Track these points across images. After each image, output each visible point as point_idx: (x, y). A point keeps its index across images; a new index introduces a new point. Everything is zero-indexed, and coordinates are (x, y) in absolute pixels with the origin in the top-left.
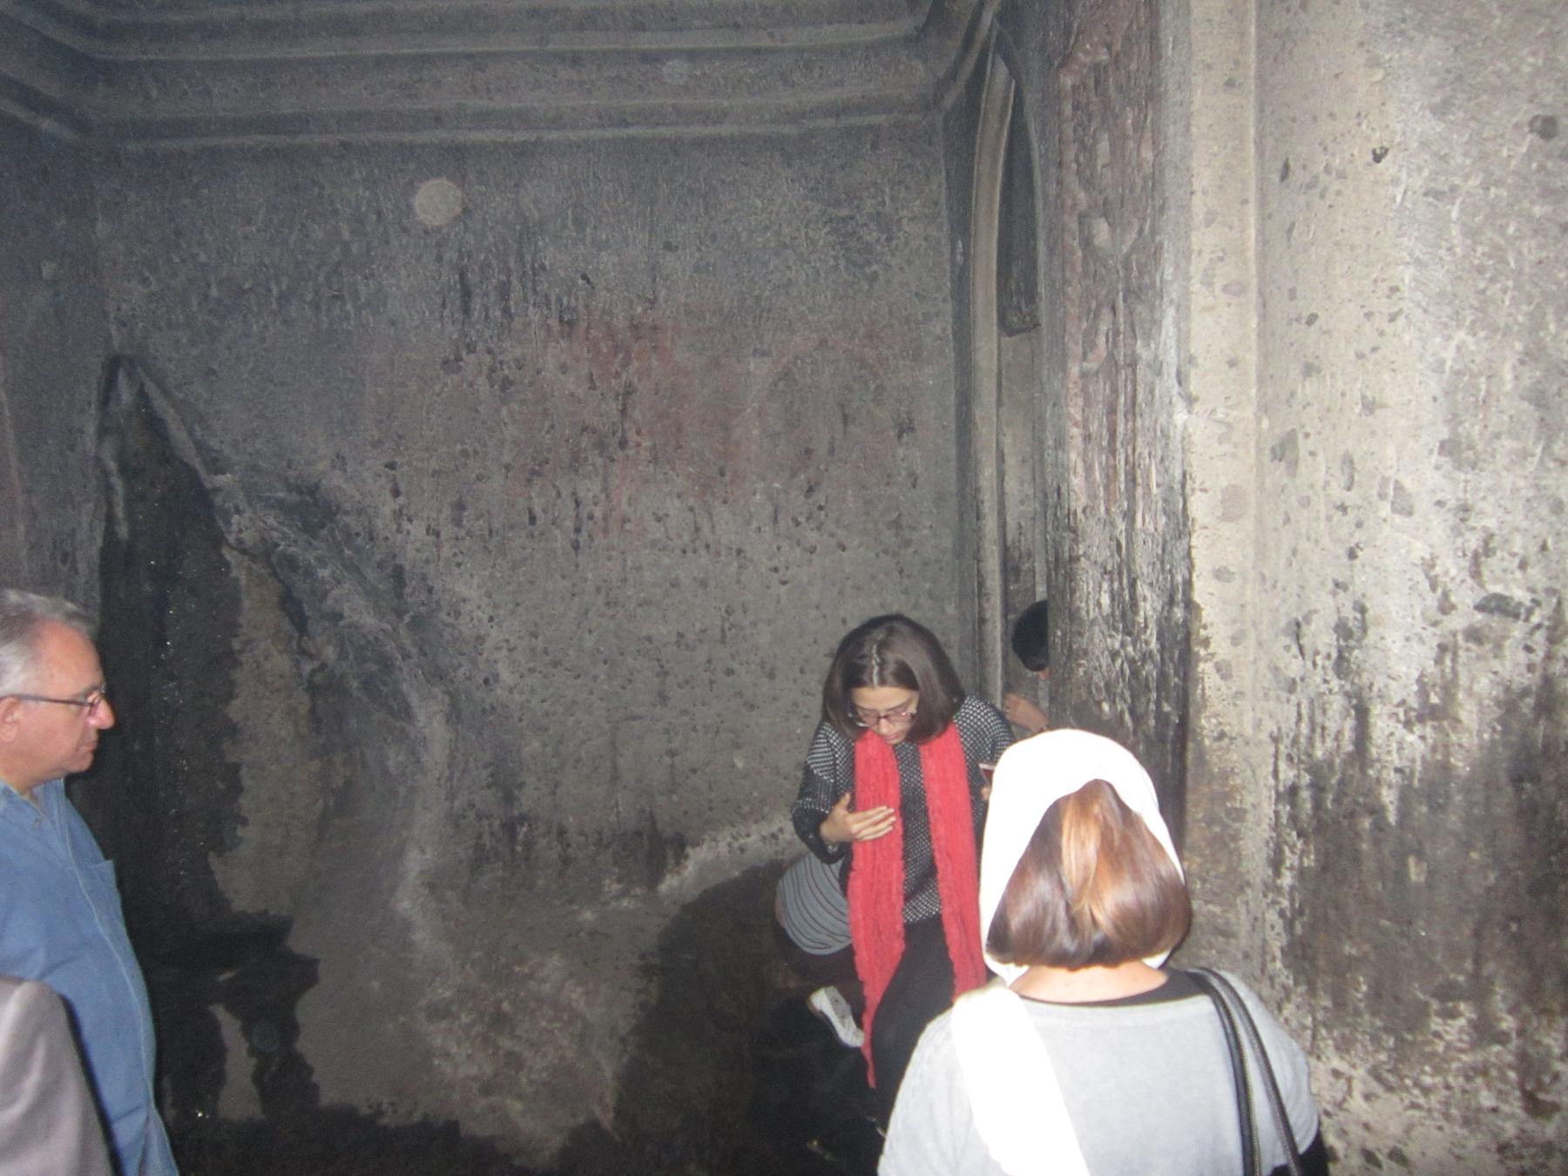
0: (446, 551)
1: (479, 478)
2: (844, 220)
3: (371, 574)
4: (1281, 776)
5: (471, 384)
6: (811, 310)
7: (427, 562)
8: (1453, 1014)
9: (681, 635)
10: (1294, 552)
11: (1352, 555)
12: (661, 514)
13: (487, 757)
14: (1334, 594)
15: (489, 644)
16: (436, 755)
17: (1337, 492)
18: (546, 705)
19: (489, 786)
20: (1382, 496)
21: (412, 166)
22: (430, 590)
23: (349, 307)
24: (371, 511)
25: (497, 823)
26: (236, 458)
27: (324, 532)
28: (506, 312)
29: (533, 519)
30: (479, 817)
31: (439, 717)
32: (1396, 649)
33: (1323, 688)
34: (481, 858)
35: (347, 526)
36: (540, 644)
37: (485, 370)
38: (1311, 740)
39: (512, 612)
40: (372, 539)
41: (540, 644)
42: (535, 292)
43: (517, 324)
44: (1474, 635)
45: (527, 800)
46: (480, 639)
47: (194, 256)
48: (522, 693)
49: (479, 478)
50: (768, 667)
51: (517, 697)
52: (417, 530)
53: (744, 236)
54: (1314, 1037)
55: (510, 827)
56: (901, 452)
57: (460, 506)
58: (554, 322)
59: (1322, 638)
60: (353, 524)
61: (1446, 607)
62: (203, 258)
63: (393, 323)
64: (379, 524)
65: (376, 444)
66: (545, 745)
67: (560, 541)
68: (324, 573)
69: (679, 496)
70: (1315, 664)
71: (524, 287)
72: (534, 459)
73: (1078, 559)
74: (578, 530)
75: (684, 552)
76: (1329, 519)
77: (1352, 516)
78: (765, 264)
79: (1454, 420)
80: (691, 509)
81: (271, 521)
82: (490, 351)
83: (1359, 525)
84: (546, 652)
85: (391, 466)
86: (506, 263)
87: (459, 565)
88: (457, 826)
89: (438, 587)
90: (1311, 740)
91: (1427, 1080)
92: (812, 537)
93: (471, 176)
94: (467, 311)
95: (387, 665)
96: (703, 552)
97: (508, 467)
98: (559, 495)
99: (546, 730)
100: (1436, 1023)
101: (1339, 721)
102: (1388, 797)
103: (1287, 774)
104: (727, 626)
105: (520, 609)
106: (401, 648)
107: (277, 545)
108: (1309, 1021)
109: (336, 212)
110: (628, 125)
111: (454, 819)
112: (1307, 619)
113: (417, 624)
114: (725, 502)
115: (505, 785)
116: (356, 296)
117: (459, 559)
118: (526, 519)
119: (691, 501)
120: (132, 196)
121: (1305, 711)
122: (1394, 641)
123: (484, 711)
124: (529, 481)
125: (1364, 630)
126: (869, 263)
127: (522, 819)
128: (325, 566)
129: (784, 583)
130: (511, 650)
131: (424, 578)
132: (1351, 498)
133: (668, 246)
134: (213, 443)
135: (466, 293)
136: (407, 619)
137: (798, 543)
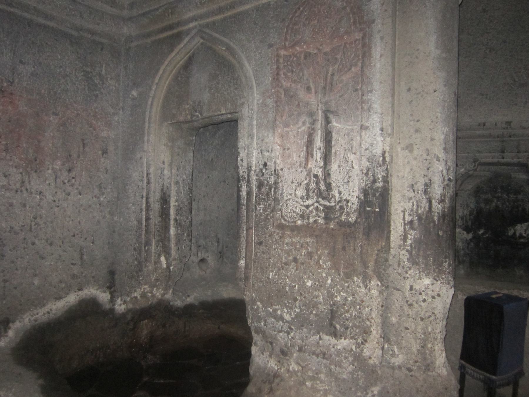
2: (88, 72)
4: (406, 219)
6: (75, 102)
8: (446, 262)
9: (12, 228)
10: (411, 170)
11: (428, 169)
12: (7, 174)
14: (424, 177)
17: (425, 156)
20: (435, 157)
32: (437, 188)
33: (421, 198)
38: (417, 210)
44: (447, 185)
50: (49, 242)
53: (52, 67)
54: (420, 275)
56: (102, 160)
59: (420, 187)
61: (444, 180)
69: (16, 167)
70: (418, 193)
73: (279, 183)
75: (17, 191)
76: (423, 162)
77: (428, 162)
78: (59, 80)
79: (445, 144)
80: (21, 173)
83: (430, 163)
90: (417, 210)
91: (443, 277)
92: (70, 188)
96: (25, 192)
100: (444, 264)
101: (425, 204)
102: (436, 219)
103: (408, 218)
104: (33, 224)
108: (418, 272)
110: (12, 7)
112: (416, 183)
114: (36, 172)
119: (21, 170)
121: (415, 204)
122: (436, 187)
125: (431, 185)
126: (96, 90)
129: (58, 207)
132: (428, 158)
133: (21, 62)
137: (64, 191)
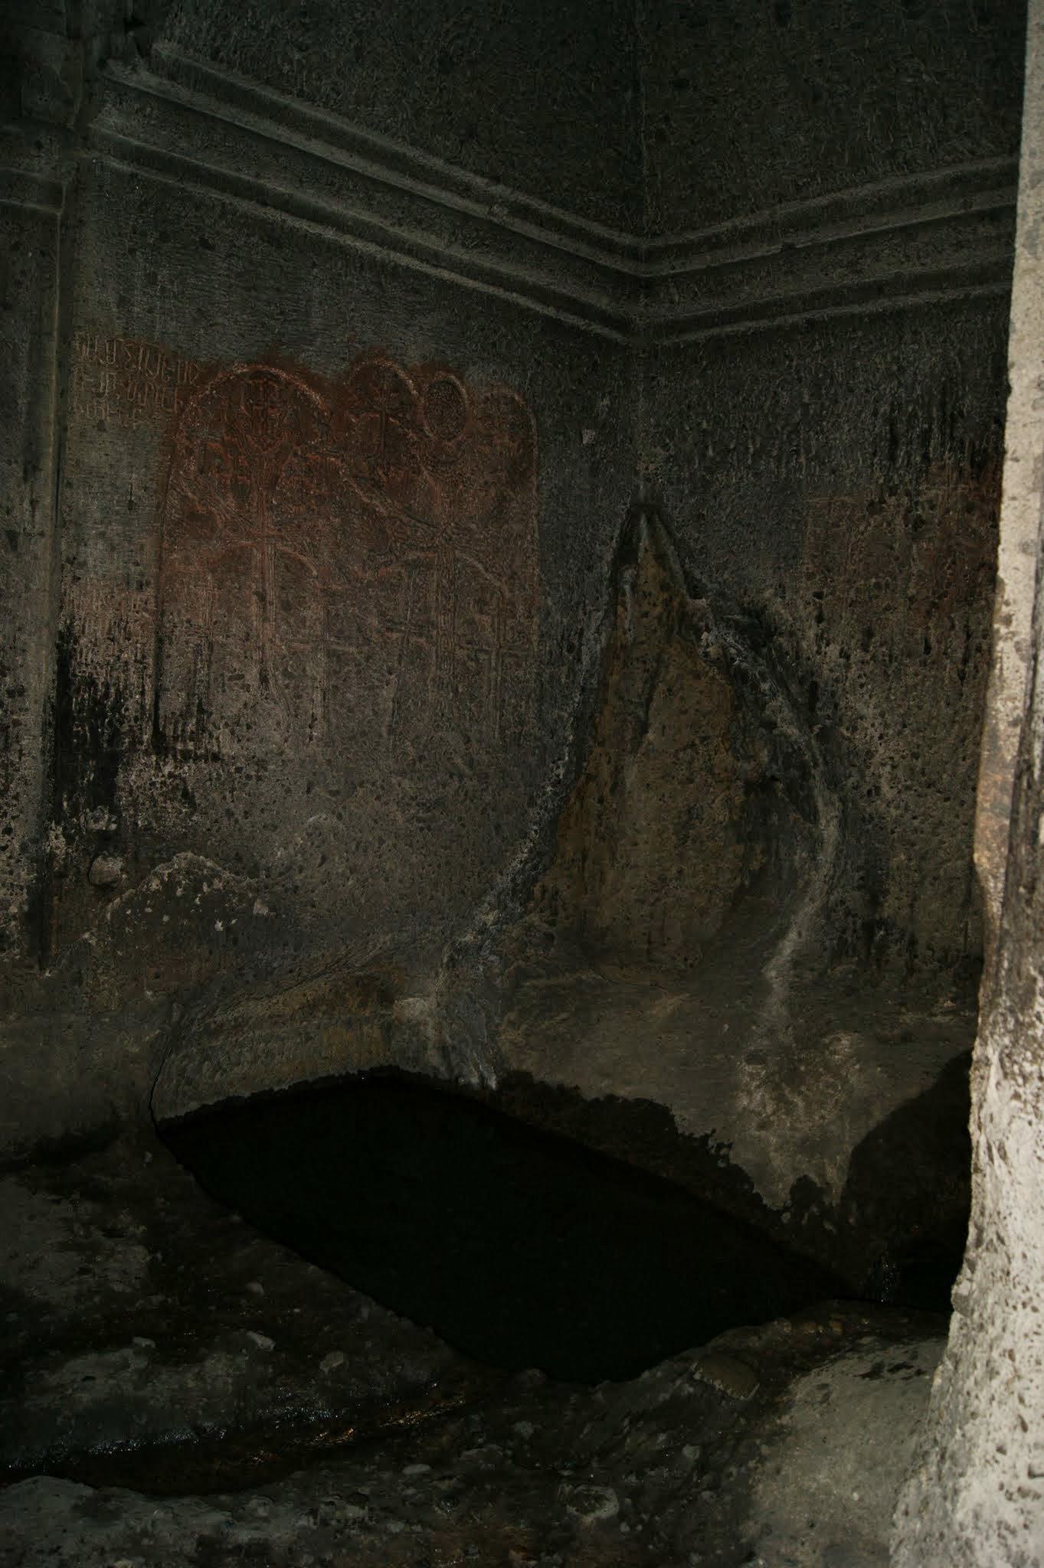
0: (853, 672)
1: (887, 609)
3: (794, 688)
5: (889, 524)
7: (837, 680)
13: (860, 862)
15: (877, 759)
16: (826, 856)
18: (916, 823)
19: (859, 888)
21: (860, 334)
22: (836, 706)
23: (802, 460)
24: (800, 634)
25: (859, 922)
26: (709, 586)
27: (765, 650)
28: (926, 457)
29: (928, 649)
30: (848, 913)
31: (835, 821)
34: (840, 952)
35: (780, 645)
36: (919, 763)
37: (902, 510)
39: (900, 733)
40: (798, 658)
41: (919, 763)
42: (952, 438)
43: (934, 469)
45: (889, 908)
46: (870, 754)
47: (700, 424)
48: (897, 807)
49: (887, 609)
51: (892, 810)
52: (833, 650)
55: (870, 928)
57: (869, 634)
58: (965, 464)
60: (785, 645)
62: (705, 425)
63: (833, 472)
64: (804, 644)
65: (810, 576)
66: (910, 859)
67: (949, 671)
68: (765, 686)
71: (943, 434)
72: (934, 593)
74: (965, 661)
81: (730, 639)
82: (908, 494)
84: (923, 773)
85: (819, 595)
86: (929, 412)
87: (862, 686)
88: (828, 917)
89: (842, 704)
93: (908, 337)
94: (893, 458)
95: (805, 775)
97: (912, 599)
98: (953, 627)
99: (913, 845)
105: (907, 731)
106: (813, 756)
107: (733, 660)
109: (800, 380)
111: (827, 911)
113: (824, 736)
115: (874, 891)
116: (808, 452)
117: (863, 680)
118: (922, 648)
120: (663, 381)
123: (864, 820)
124: (929, 613)
127: (881, 923)
128: (764, 681)
130: (894, 767)
131: (833, 694)
134: (697, 574)
135: (894, 442)
136: (816, 729)
